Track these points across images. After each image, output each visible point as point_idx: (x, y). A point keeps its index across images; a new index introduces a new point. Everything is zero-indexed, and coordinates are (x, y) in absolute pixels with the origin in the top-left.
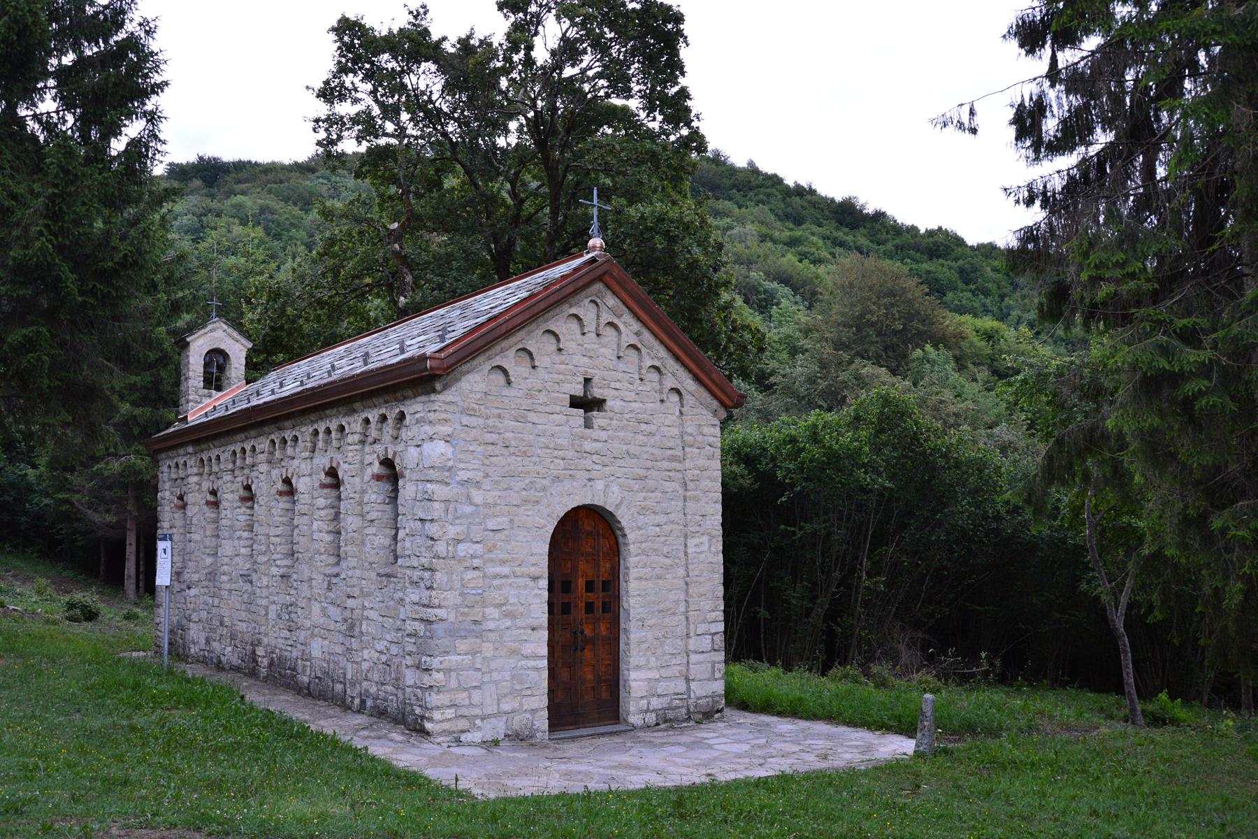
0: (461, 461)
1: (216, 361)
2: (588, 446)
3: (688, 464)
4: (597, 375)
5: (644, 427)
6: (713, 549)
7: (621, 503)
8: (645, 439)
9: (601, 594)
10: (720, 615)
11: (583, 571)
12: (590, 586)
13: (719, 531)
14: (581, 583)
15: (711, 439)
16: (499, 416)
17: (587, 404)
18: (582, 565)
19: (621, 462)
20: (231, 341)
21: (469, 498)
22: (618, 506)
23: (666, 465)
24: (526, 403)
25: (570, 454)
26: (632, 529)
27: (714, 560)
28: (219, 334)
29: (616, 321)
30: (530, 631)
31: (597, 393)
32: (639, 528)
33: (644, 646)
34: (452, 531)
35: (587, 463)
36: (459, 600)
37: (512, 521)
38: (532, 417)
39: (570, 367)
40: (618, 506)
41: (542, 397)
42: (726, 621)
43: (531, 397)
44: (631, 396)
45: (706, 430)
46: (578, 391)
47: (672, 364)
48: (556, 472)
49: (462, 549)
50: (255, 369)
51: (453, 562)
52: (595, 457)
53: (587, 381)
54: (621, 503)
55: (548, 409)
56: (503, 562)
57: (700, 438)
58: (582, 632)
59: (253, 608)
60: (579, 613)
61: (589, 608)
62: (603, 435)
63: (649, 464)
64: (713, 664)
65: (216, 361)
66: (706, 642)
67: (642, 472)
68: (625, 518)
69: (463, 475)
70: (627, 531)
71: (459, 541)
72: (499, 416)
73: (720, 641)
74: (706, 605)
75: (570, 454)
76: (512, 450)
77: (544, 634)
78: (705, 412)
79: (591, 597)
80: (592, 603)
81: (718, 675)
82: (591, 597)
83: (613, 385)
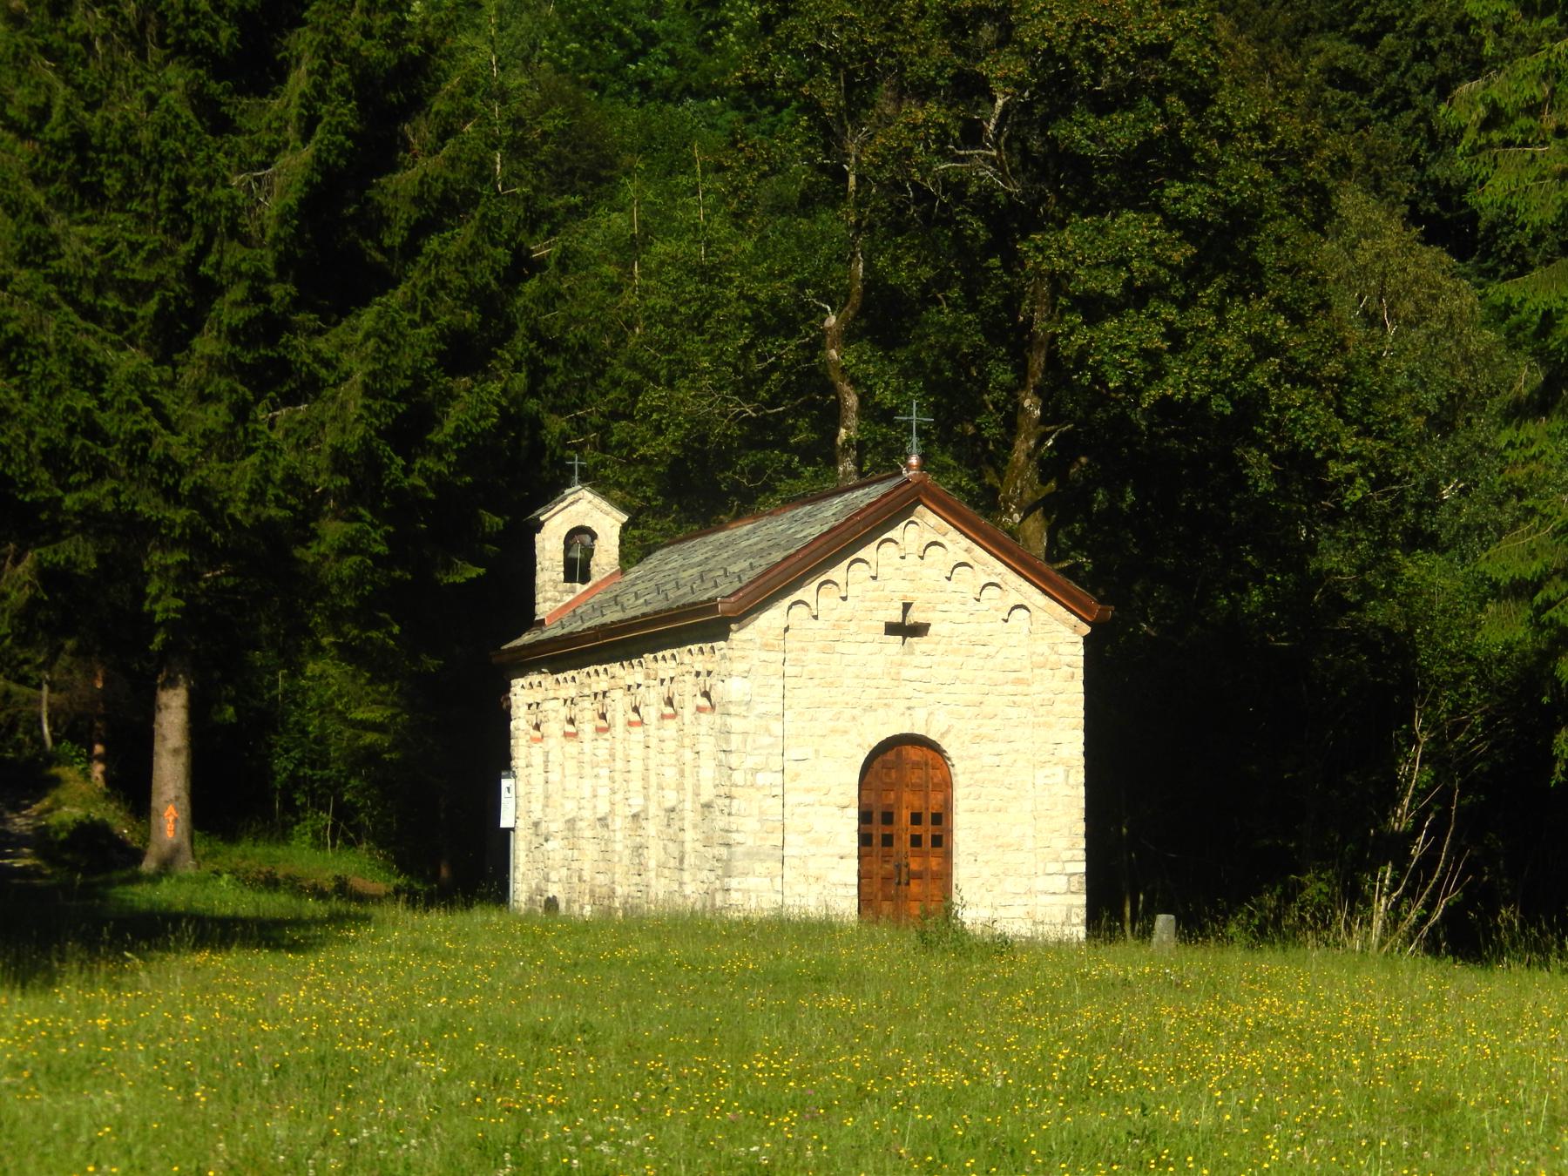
0: (759, 695)
1: (581, 539)
2: (906, 673)
3: (1034, 688)
4: (919, 600)
5: (979, 649)
6: (1071, 781)
7: (948, 731)
8: (981, 662)
9: (931, 827)
10: (1082, 855)
11: (908, 803)
12: (916, 819)
13: (1080, 761)
14: (905, 815)
15: (1068, 659)
16: (803, 649)
17: (906, 630)
18: (907, 796)
19: (952, 689)
20: (597, 515)
21: (767, 730)
22: (943, 735)
23: (1010, 689)
24: (834, 634)
25: (886, 682)
26: (961, 758)
27: (1073, 793)
28: (582, 506)
29: (940, 539)
30: (836, 859)
31: (915, 617)
32: (972, 758)
33: (978, 882)
34: (750, 763)
35: (907, 690)
36: (757, 826)
37: (817, 751)
38: (839, 647)
39: (886, 592)
40: (943, 735)
41: (852, 626)
42: (1089, 860)
43: (839, 627)
44: (964, 618)
45: (1062, 649)
46: (896, 617)
47: (1012, 579)
48: (867, 703)
49: (761, 779)
50: (634, 549)
51: (752, 791)
52: (916, 685)
53: (907, 607)
54: (948, 731)
55: (860, 638)
56: (808, 791)
57: (1054, 658)
58: (907, 865)
59: (608, 856)
60: (903, 845)
61: (916, 841)
62: (927, 661)
63: (986, 689)
64: (1070, 908)
65: (581, 539)
66: (1060, 883)
67: (979, 698)
68: (950, 746)
69: (760, 709)
70: (954, 761)
71: (757, 771)
72: (803, 649)
73: (1080, 883)
74: (1060, 843)
75: (886, 682)
76: (816, 681)
77: (854, 864)
78: (1062, 628)
79: (918, 830)
80: (919, 837)
81: (1075, 920)
82: (918, 830)
83: (939, 607)
